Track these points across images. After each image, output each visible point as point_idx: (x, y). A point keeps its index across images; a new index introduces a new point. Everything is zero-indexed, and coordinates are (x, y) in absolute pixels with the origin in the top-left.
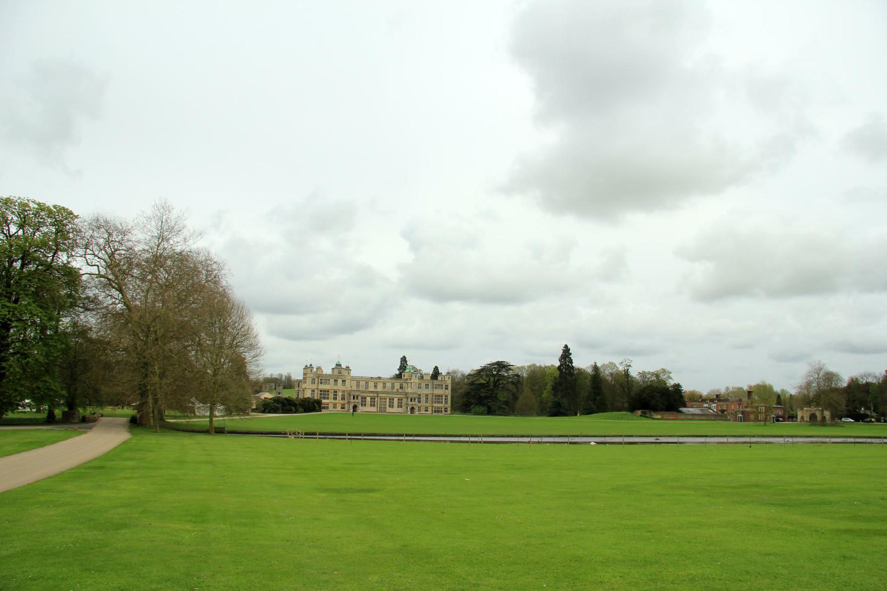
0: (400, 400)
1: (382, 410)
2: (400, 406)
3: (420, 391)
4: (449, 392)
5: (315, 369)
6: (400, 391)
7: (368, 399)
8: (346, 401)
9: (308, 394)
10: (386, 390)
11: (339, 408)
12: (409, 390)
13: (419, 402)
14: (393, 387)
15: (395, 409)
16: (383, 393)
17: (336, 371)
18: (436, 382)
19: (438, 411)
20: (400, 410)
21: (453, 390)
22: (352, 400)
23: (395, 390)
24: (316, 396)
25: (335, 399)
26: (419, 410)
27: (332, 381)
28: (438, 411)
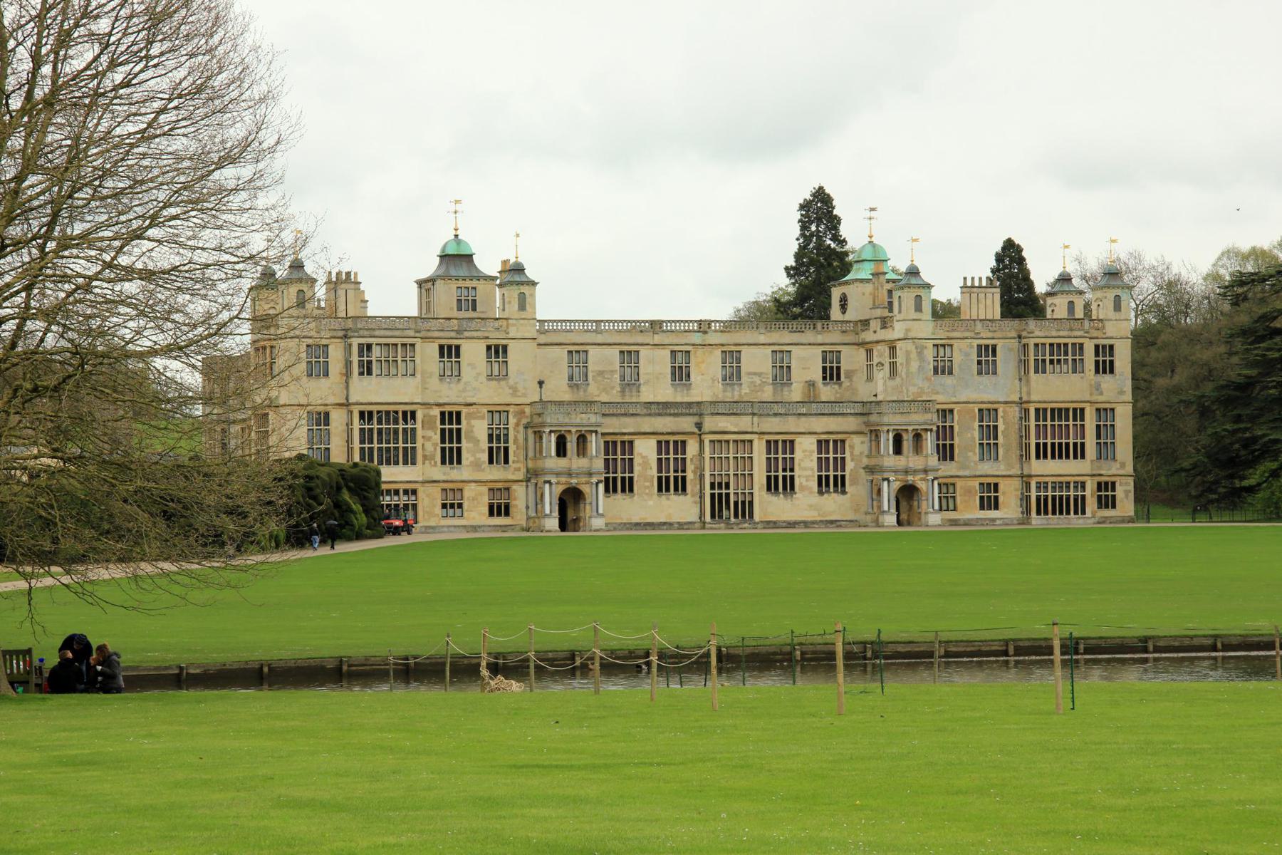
0: (831, 447)
1: (727, 505)
2: (831, 482)
3: (946, 391)
4: (1117, 389)
5: (321, 291)
6: (827, 392)
7: (646, 450)
8: (514, 471)
9: (292, 439)
10: (744, 390)
11: (476, 512)
12: (881, 386)
13: (946, 452)
14: (783, 373)
15: (806, 503)
16: (734, 409)
17: (446, 296)
18: (1037, 331)
19: (1059, 502)
20: (833, 505)
21: (1140, 385)
23: (796, 393)
24: (341, 449)
25: (451, 456)
26: (948, 500)
27: (427, 354)
28: (1059, 502)
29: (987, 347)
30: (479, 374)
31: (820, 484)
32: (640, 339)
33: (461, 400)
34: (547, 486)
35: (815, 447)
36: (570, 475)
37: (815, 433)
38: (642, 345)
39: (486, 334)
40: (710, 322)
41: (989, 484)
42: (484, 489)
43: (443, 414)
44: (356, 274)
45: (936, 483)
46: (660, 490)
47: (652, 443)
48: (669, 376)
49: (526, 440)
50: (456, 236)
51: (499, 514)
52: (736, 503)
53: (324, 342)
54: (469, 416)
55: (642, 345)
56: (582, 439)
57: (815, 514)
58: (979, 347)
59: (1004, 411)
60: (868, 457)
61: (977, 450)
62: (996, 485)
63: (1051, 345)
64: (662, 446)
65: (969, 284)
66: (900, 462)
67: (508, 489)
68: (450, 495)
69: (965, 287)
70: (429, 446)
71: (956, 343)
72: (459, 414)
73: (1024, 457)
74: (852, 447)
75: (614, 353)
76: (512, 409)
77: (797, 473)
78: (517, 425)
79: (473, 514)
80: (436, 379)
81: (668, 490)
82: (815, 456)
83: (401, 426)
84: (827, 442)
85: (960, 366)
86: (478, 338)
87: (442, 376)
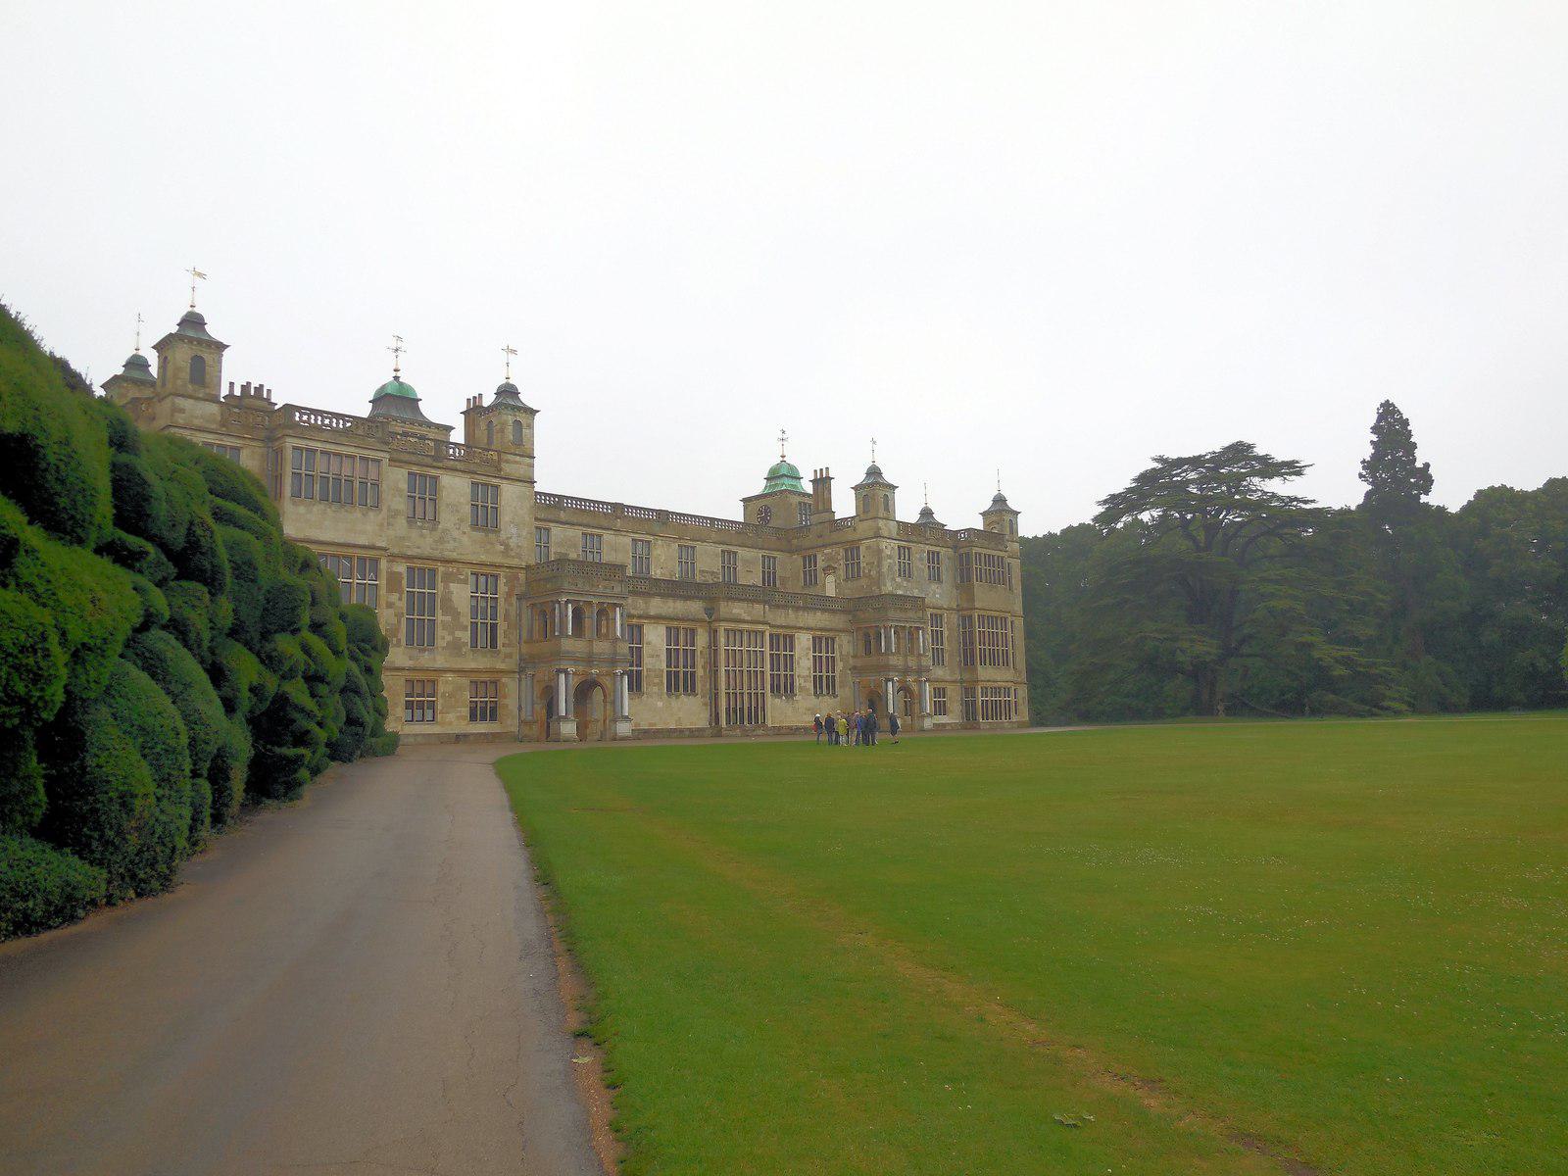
22: (569, 645)
31: (815, 687)
33: (437, 554)
34: (562, 677)
36: (590, 659)
37: (811, 629)
39: (472, 467)
42: (465, 681)
44: (269, 391)
46: (669, 688)
47: (662, 630)
49: (520, 615)
50: (396, 378)
51: (483, 719)
52: (750, 709)
53: (237, 443)
54: (448, 578)
56: (602, 612)
60: (855, 656)
64: (672, 635)
67: (495, 683)
68: (418, 689)
72: (433, 572)
73: (968, 660)
74: (840, 646)
76: (502, 573)
77: (797, 671)
78: (509, 595)
79: (451, 716)
80: (402, 521)
81: (677, 689)
82: (811, 654)
84: (820, 638)
86: (463, 472)
87: (411, 519)
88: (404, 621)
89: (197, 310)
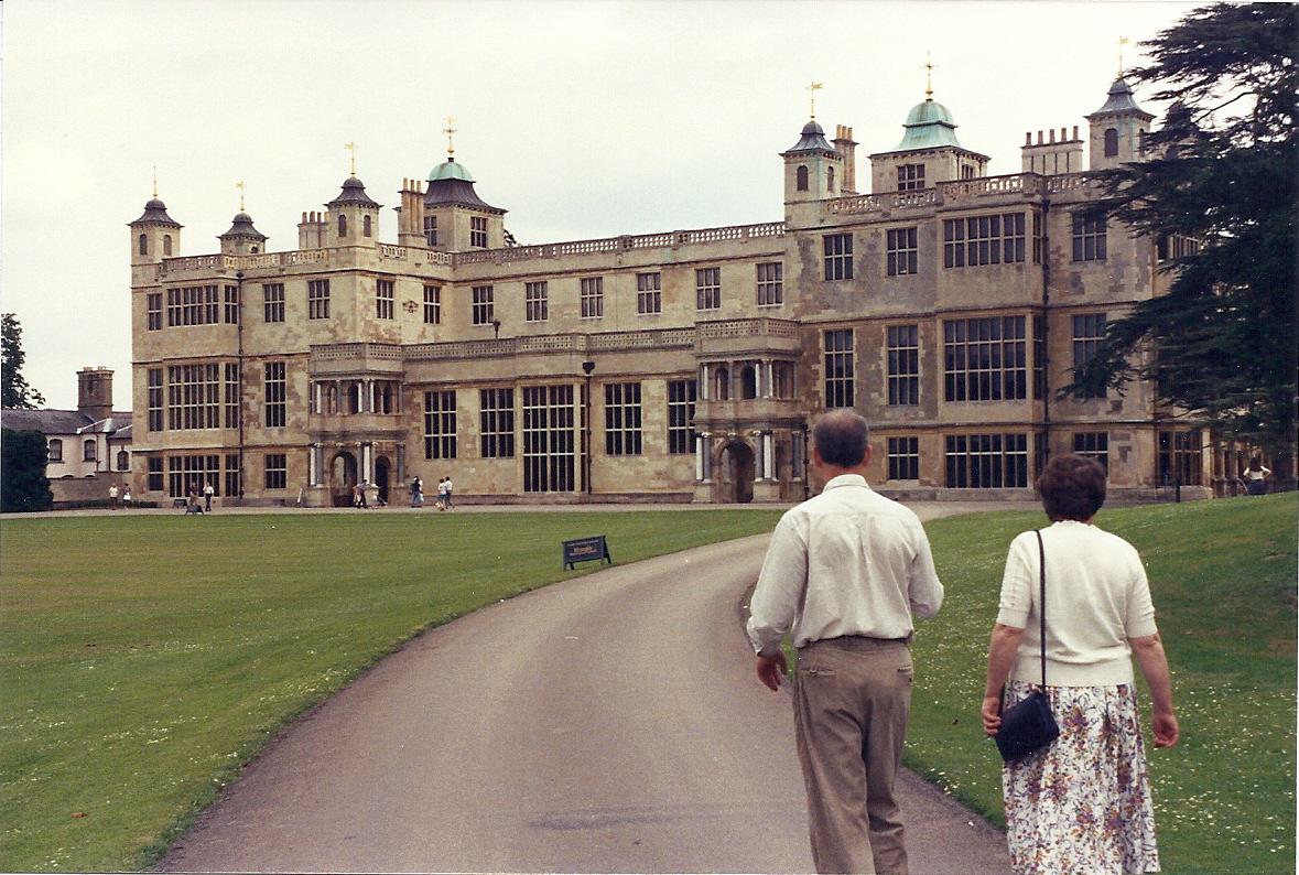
7: (469, 404)
25: (276, 417)
29: (901, 231)
30: (302, 317)
32: (600, 262)
35: (664, 392)
38: (604, 270)
40: (687, 233)
41: (903, 440)
43: (268, 365)
45: (767, 438)
48: (636, 306)
50: (451, 160)
55: (604, 270)
57: (665, 484)
58: (890, 232)
59: (925, 328)
61: (885, 388)
62: (914, 441)
63: (970, 220)
65: (1034, 141)
66: (728, 412)
69: (1028, 146)
70: (253, 405)
71: (855, 232)
75: (573, 283)
83: (205, 383)
85: (861, 266)
88: (263, 408)
89: (159, 198)
